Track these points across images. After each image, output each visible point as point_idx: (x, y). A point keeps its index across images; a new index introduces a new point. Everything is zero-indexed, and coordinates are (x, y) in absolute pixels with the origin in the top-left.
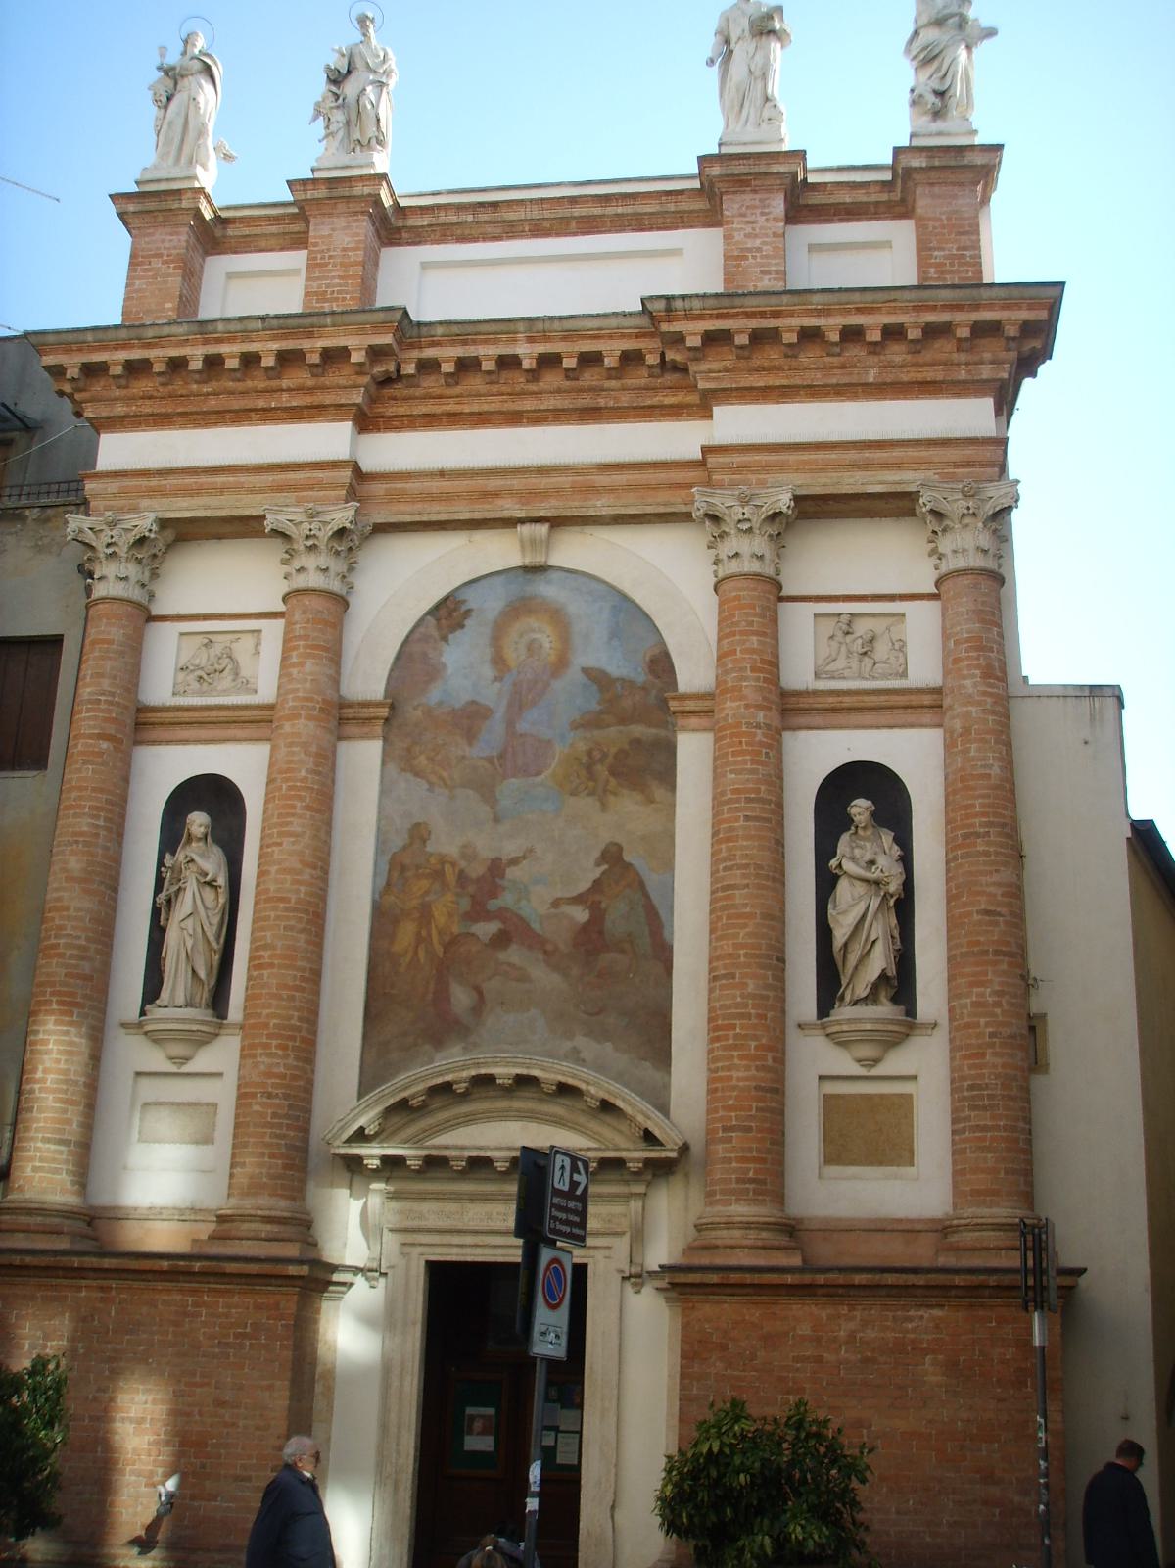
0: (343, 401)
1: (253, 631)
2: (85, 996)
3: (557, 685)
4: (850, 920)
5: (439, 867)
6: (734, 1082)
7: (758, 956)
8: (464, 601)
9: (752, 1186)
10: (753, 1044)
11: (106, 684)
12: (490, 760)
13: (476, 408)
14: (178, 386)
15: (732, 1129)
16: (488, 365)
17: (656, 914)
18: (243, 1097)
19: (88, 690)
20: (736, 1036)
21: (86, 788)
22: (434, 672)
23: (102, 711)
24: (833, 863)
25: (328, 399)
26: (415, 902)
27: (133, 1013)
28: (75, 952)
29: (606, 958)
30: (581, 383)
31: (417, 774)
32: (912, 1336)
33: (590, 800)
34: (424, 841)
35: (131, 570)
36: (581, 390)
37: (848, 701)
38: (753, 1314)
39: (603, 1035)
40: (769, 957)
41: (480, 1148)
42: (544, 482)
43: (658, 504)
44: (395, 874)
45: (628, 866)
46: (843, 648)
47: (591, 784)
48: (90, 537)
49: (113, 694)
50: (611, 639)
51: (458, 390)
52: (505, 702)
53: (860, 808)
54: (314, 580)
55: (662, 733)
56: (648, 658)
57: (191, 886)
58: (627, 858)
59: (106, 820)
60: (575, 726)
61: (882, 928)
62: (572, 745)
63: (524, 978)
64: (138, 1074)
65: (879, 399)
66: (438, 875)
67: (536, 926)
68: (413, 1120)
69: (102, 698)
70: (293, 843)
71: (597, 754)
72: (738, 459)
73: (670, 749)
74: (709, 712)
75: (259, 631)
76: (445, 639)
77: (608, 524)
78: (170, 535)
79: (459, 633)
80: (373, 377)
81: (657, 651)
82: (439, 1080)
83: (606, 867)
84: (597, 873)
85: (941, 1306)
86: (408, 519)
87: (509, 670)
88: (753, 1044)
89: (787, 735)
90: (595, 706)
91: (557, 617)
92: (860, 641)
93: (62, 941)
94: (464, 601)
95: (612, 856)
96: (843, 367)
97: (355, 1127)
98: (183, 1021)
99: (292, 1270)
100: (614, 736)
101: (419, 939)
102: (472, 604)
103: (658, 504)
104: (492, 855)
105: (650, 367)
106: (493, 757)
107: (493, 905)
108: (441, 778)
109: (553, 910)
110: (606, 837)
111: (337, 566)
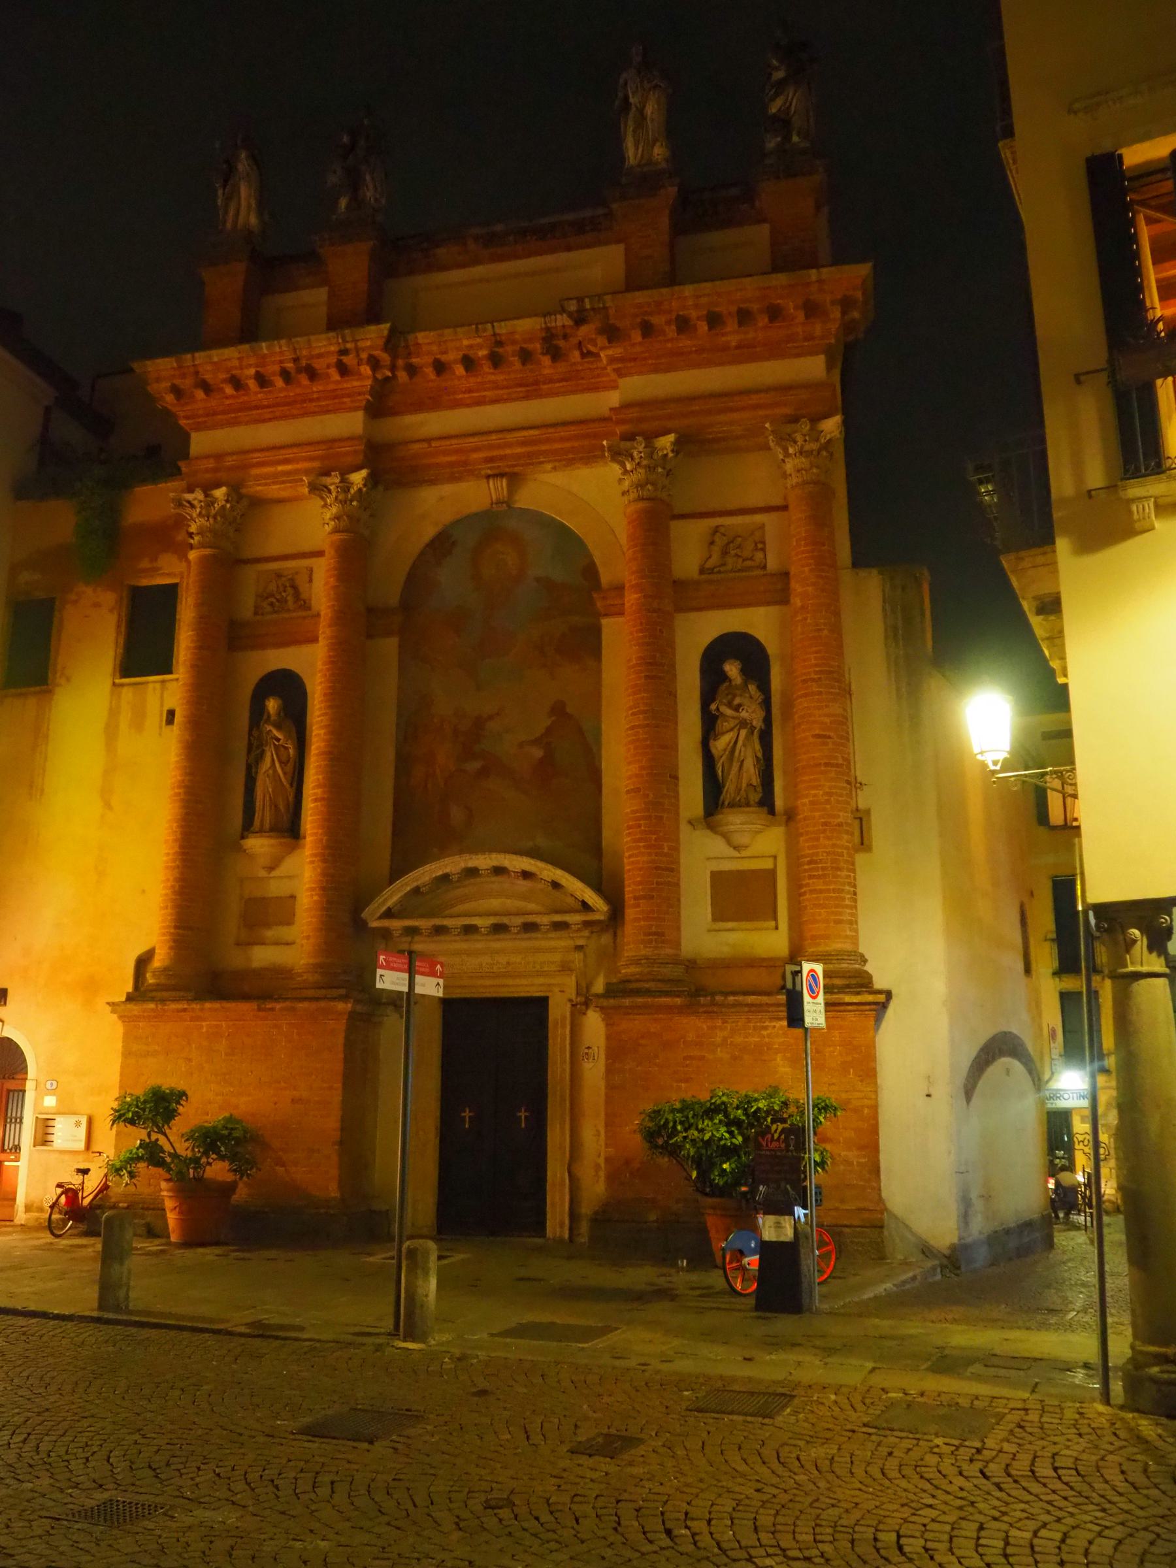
24: (713, 707)
53: (732, 669)
58: (569, 710)
73: (597, 631)
83: (553, 718)
84: (548, 722)
95: (558, 710)
97: (384, 908)
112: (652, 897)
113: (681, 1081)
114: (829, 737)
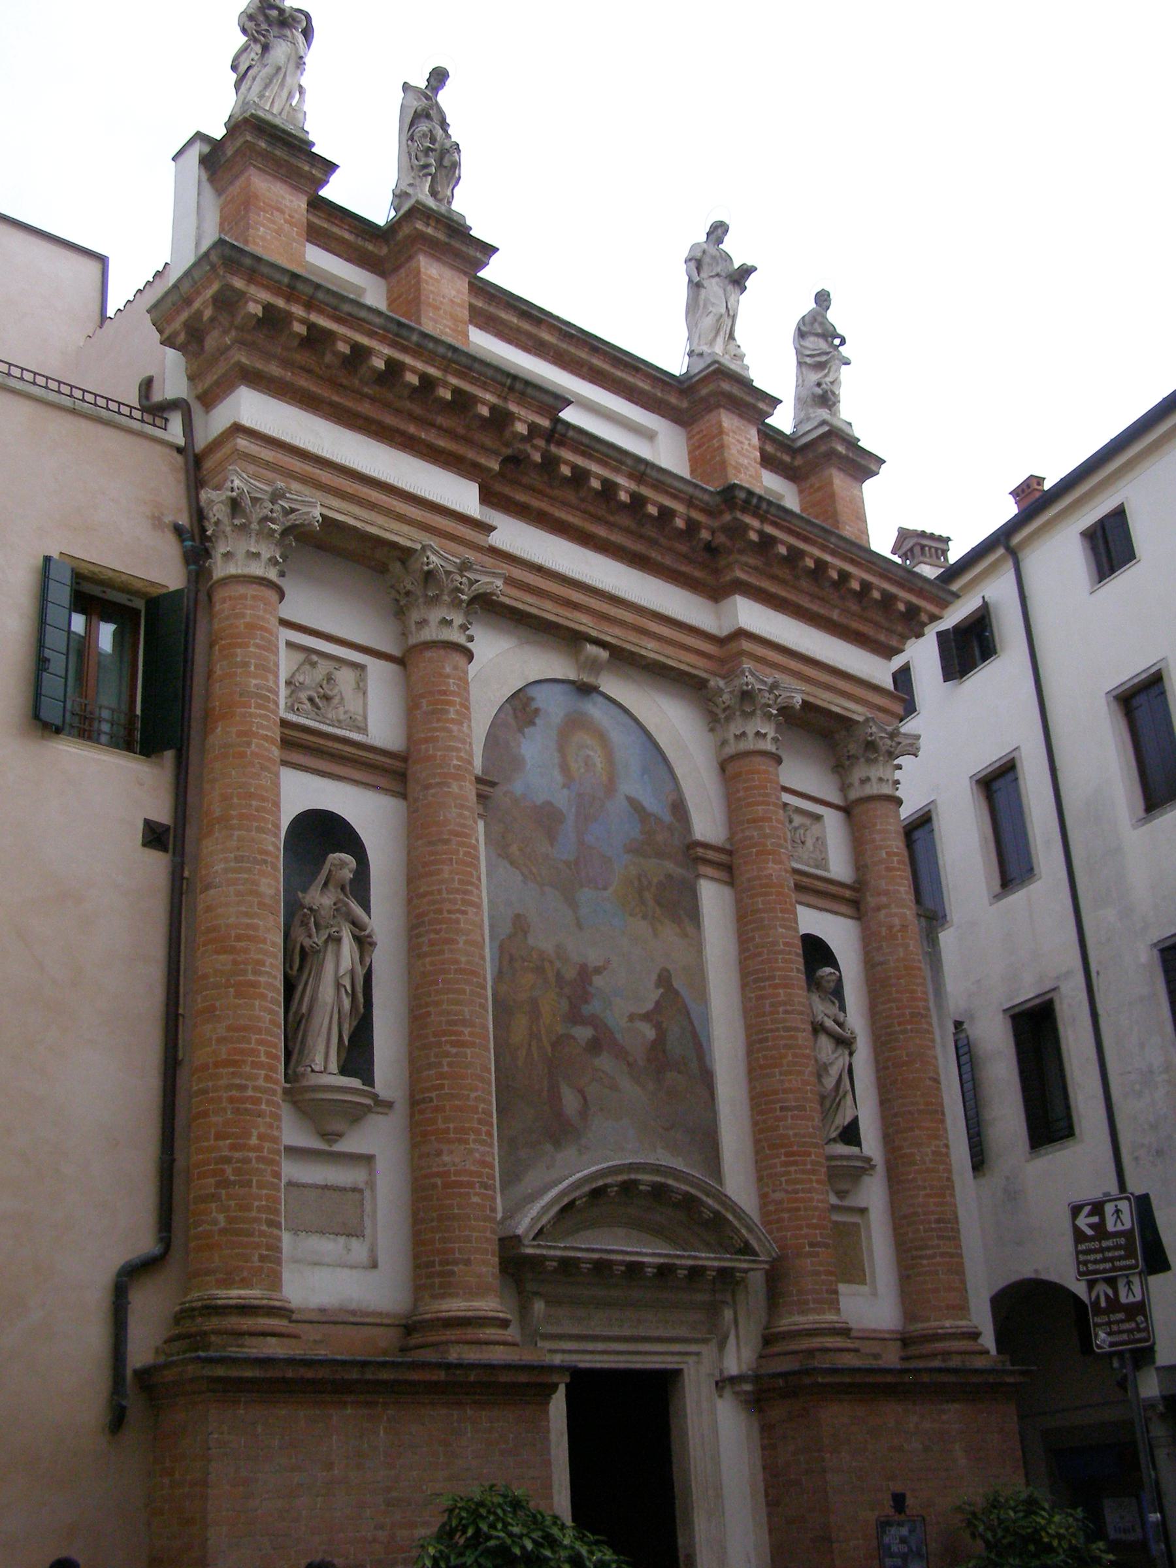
22: (517, 763)
29: (671, 1075)
34: (525, 933)
45: (677, 993)
51: (556, 493)
66: (539, 970)
67: (618, 1036)
72: (760, 651)
76: (520, 730)
83: (661, 990)
96: (822, 599)
108: (531, 872)
109: (629, 1024)
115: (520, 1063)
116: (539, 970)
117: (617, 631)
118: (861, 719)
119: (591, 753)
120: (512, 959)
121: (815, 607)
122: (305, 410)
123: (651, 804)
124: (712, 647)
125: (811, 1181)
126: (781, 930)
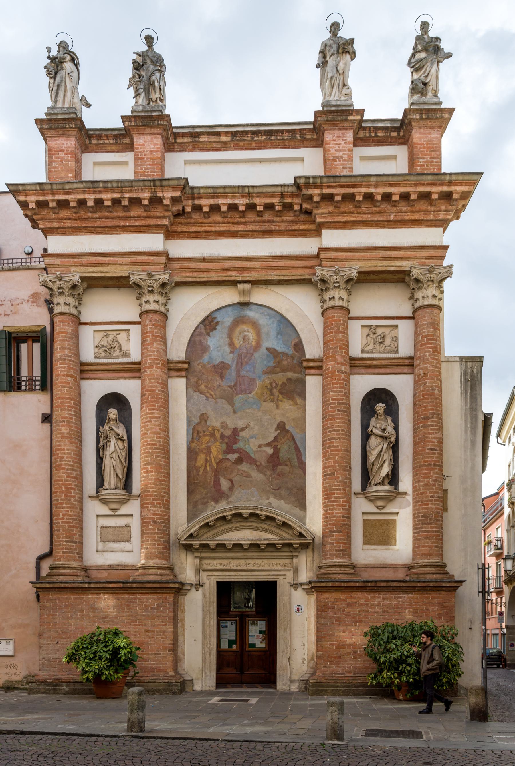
0: (159, 223)
1: (125, 330)
2: (75, 485)
3: (256, 355)
4: (375, 453)
5: (212, 432)
6: (335, 515)
7: (343, 466)
8: (216, 318)
9: (341, 552)
10: (342, 500)
11: (66, 352)
12: (230, 387)
13: (217, 229)
14: (82, 214)
15: (334, 532)
16: (224, 209)
17: (299, 451)
18: (144, 523)
19: (59, 355)
20: (335, 497)
21: (64, 398)
22: (205, 349)
23: (66, 364)
24: (369, 430)
25: (152, 222)
26: (204, 446)
27: (93, 492)
28: (69, 467)
29: (280, 468)
30: (264, 218)
31: (201, 393)
32: (401, 603)
33: (272, 404)
34: (206, 421)
35: (70, 300)
36: (264, 222)
37: (375, 362)
38: (343, 596)
39: (280, 497)
40: (346, 466)
41: (238, 540)
42: (249, 264)
43: (298, 275)
44: (195, 435)
45: (288, 431)
46: (372, 340)
47: (272, 397)
48: (50, 285)
49: (70, 357)
50: (277, 335)
51: (209, 220)
52: (235, 362)
54: (153, 306)
55: (300, 376)
56: (293, 344)
57: (113, 440)
59: (75, 412)
60: (265, 373)
61: (387, 456)
62: (263, 381)
63: (248, 476)
64: (98, 516)
65: (394, 228)
66: (212, 435)
67: (252, 455)
68: (210, 531)
69: (66, 358)
70: (156, 421)
71: (274, 385)
73: (303, 383)
74: (320, 367)
75: (129, 330)
76: (208, 334)
77: (275, 284)
78: (85, 284)
79: (214, 332)
80: (172, 213)
81: (296, 340)
82: (220, 515)
83: (279, 431)
84: (276, 434)
85: (412, 593)
86: (190, 280)
87: (236, 349)
88: (342, 500)
89: (352, 377)
90: (272, 364)
91: (254, 324)
92: (379, 337)
93: (63, 463)
94: (216, 318)
95: (281, 427)
96: (380, 212)
97: (189, 533)
98: (116, 494)
99: (172, 585)
100: (280, 378)
101: (206, 461)
102: (219, 319)
103: (298, 275)
104: (234, 427)
105: (296, 211)
106: (232, 386)
107: (235, 447)
108: (211, 394)
110: (279, 419)
111: (162, 300)
112: (340, 532)
113: (356, 622)
114: (436, 450)
115: (201, 473)
116: (212, 435)
117: (253, 273)
118: (408, 268)
119: (247, 333)
120: (198, 432)
121: (377, 218)
122: (76, 235)
123: (280, 348)
124: (313, 261)
125: (334, 505)
126: (331, 393)
